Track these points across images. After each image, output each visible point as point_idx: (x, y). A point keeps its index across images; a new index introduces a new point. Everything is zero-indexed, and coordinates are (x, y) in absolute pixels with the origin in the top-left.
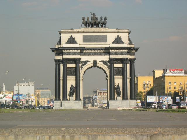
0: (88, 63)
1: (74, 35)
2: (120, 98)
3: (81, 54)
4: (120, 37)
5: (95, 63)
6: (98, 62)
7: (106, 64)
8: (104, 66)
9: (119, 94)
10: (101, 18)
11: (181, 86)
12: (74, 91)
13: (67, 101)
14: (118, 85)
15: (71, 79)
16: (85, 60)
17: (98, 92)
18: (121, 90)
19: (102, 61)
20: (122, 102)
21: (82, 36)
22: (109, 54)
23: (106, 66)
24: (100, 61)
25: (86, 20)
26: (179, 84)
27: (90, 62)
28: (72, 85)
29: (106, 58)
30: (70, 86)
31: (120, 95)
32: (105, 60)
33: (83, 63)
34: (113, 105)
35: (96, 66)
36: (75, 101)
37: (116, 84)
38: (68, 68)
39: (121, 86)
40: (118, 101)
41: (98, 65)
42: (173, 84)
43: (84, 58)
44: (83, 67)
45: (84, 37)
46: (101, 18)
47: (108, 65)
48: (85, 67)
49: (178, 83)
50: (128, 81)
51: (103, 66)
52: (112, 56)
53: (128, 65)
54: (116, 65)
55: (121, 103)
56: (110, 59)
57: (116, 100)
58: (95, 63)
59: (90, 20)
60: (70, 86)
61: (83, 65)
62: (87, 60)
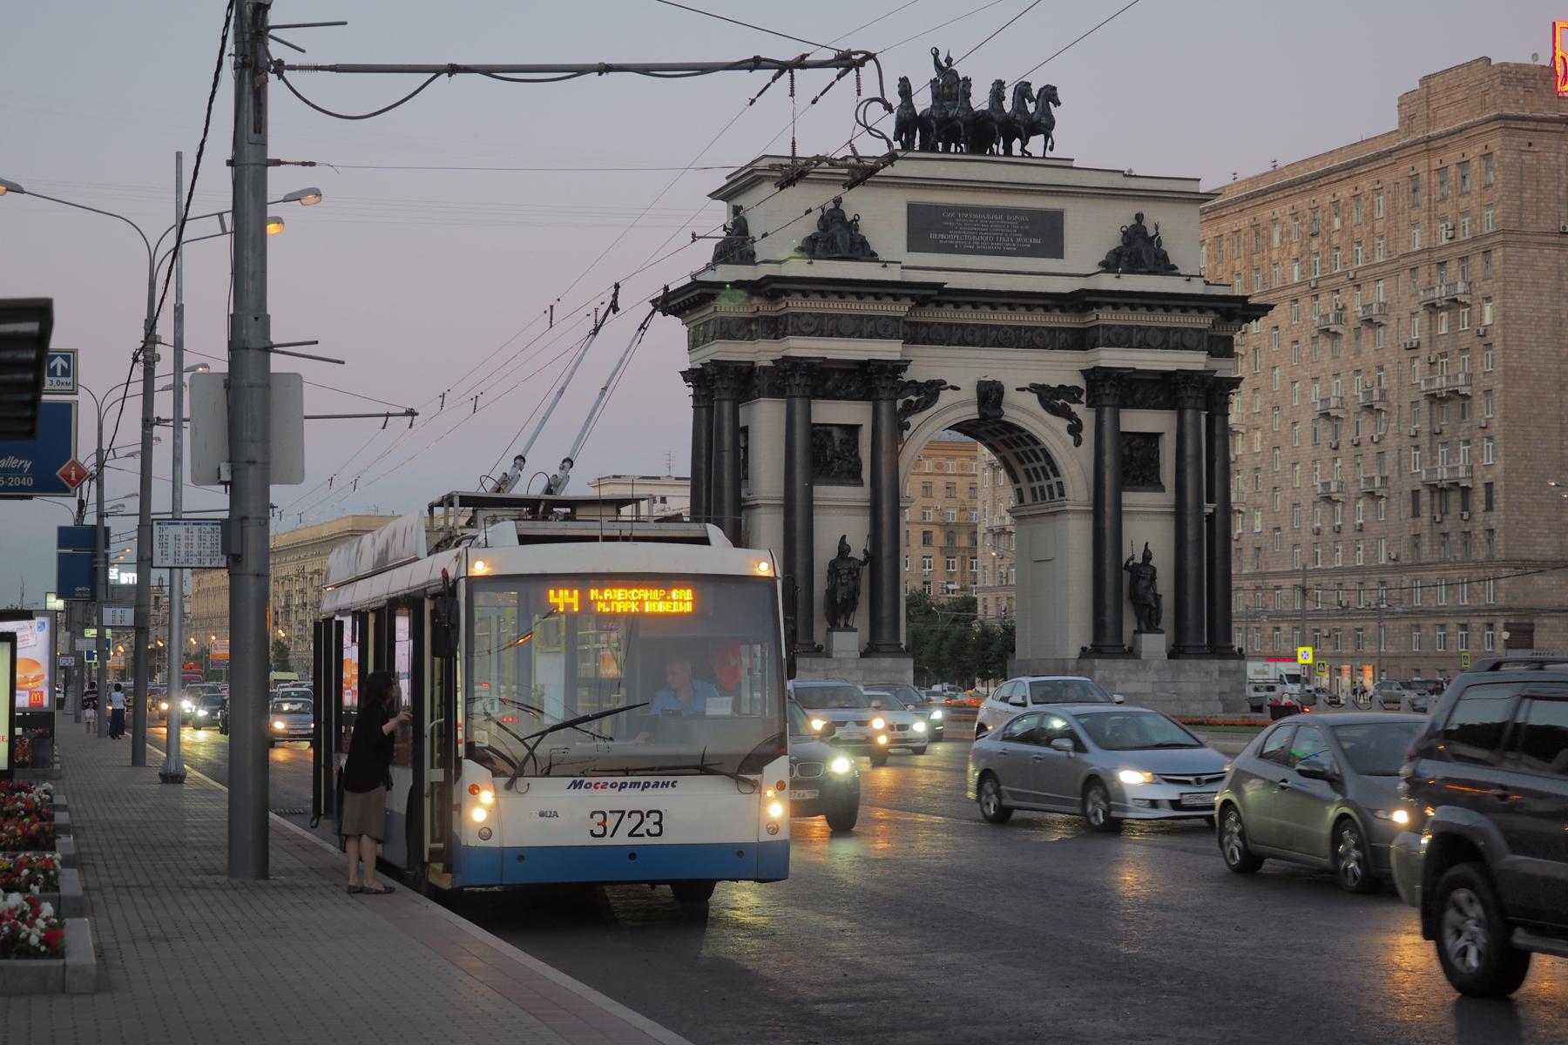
0: (945, 397)
1: (858, 203)
2: (1154, 645)
3: (916, 334)
4: (1151, 233)
5: (990, 395)
6: (1010, 395)
7: (1063, 412)
9: (1149, 620)
12: (855, 592)
14: (1147, 556)
19: (1036, 389)
22: (1081, 340)
23: (1062, 424)
28: (843, 548)
29: (1062, 368)
30: (833, 554)
31: (1158, 621)
32: (1054, 385)
33: (914, 399)
36: (867, 662)
37: (1132, 549)
41: (1011, 415)
43: (927, 363)
44: (914, 420)
45: (912, 208)
47: (1068, 414)
58: (990, 395)
60: (834, 554)
61: (911, 409)
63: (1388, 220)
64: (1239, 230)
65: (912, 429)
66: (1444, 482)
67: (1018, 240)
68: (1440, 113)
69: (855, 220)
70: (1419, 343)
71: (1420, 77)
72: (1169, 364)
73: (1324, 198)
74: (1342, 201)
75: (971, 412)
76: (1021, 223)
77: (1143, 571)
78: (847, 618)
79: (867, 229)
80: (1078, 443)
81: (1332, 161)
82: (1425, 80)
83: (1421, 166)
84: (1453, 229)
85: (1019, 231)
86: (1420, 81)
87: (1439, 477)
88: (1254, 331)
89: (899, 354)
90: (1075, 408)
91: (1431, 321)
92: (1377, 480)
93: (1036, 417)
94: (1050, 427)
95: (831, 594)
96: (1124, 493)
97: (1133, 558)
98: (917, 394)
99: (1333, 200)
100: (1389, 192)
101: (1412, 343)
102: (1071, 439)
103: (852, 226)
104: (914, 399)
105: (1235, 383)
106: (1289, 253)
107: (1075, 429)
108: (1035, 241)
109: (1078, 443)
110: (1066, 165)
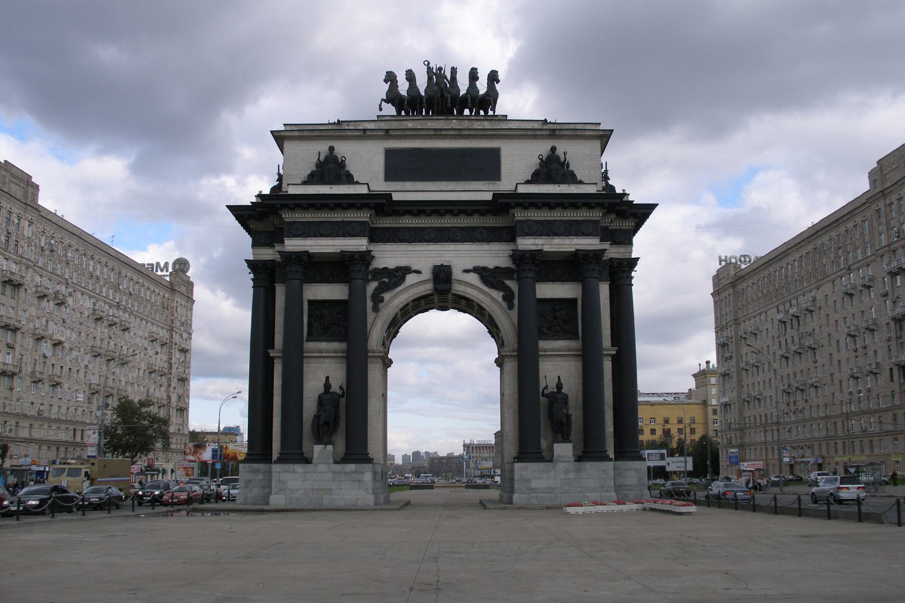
0: (411, 279)
1: (343, 149)
2: (564, 450)
4: (562, 159)
5: (442, 275)
6: (457, 274)
8: (488, 295)
9: (561, 431)
10: (473, 75)
11: (667, 426)
12: (337, 416)
13: (299, 468)
14: (559, 386)
15: (321, 356)
16: (391, 264)
17: (473, 447)
18: (575, 413)
19: (476, 270)
20: (578, 471)
21: (383, 150)
22: (508, 235)
23: (498, 295)
24: (466, 271)
25: (403, 87)
26: (662, 422)
27: (418, 272)
28: (327, 386)
33: (386, 280)
34: (534, 484)
35: (450, 289)
36: (338, 467)
38: (310, 302)
39: (572, 387)
40: (561, 466)
41: (458, 288)
42: (648, 422)
44: (387, 296)
46: (473, 75)
48: (395, 300)
49: (660, 420)
50: (607, 365)
51: (482, 291)
52: (526, 243)
53: (604, 290)
54: (548, 290)
55: (572, 475)
56: (519, 257)
57: (551, 461)
58: (442, 275)
59: (422, 83)
62: (403, 262)
63: (870, 235)
64: (809, 252)
65: (385, 302)
66: (903, 362)
68: (888, 176)
69: (342, 162)
70: (887, 293)
71: (877, 161)
73: (842, 229)
74: (850, 229)
77: (557, 398)
78: (331, 435)
79: (351, 167)
81: (844, 212)
82: (878, 162)
83: (881, 204)
84: (898, 232)
86: (877, 162)
87: (901, 360)
88: (818, 299)
89: (365, 247)
90: (508, 283)
91: (892, 281)
92: (874, 364)
93: (476, 288)
94: (488, 295)
95: (317, 417)
96: (543, 344)
97: (546, 387)
98: (388, 277)
99: (846, 229)
100: (869, 221)
101: (884, 293)
102: (504, 304)
103: (342, 165)
104: (386, 280)
105: (633, 262)
106: (830, 259)
107: (508, 298)
109: (511, 307)
110: (504, 118)
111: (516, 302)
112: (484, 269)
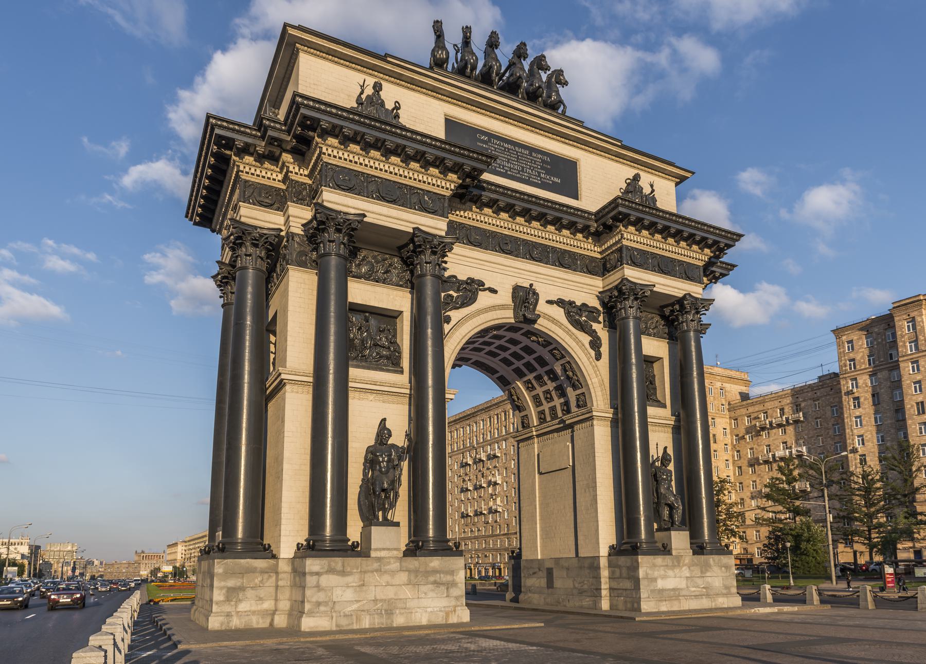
0: (484, 299)
19: (560, 303)
23: (586, 339)
24: (550, 302)
27: (493, 291)
33: (455, 295)
44: (455, 315)
65: (452, 323)
67: (542, 176)
72: (676, 290)
75: (508, 316)
76: (543, 161)
80: (598, 357)
85: (542, 168)
98: (458, 291)
102: (593, 353)
104: (455, 295)
107: (595, 344)
108: (556, 180)
109: (598, 357)
111: (605, 349)
112: (571, 303)
